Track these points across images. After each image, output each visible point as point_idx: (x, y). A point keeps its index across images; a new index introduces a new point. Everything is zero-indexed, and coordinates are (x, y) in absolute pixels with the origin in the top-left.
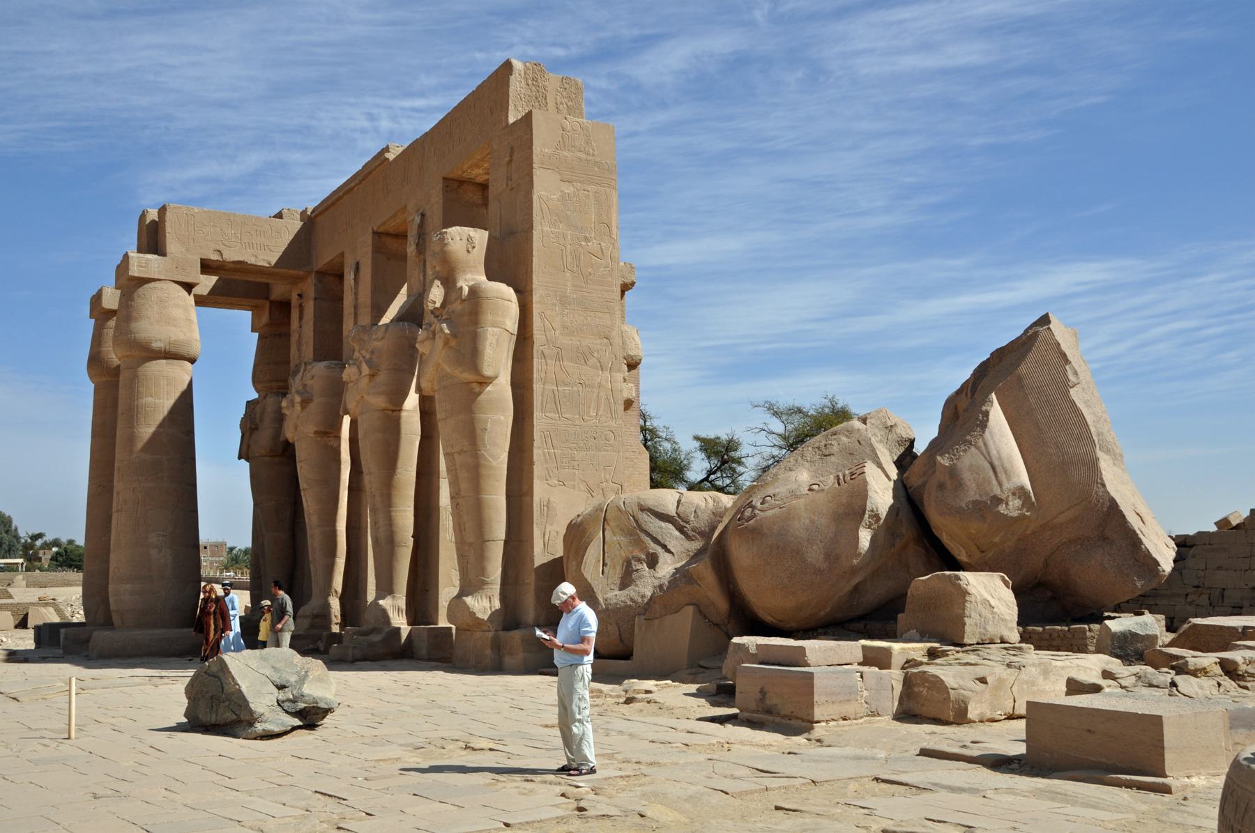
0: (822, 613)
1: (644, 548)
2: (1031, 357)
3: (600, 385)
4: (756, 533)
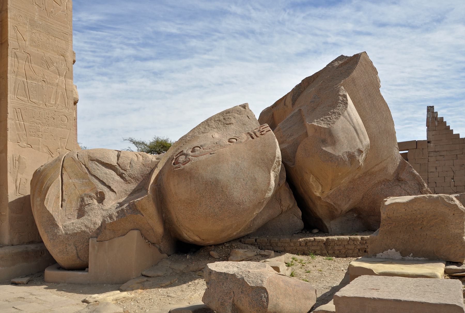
0: (235, 234)
1: (94, 188)
2: (358, 67)
3: (58, 85)
4: (189, 175)
